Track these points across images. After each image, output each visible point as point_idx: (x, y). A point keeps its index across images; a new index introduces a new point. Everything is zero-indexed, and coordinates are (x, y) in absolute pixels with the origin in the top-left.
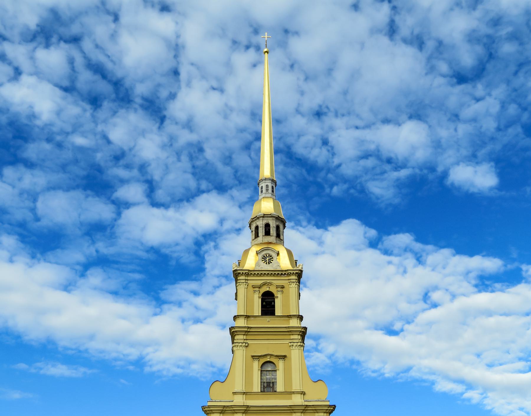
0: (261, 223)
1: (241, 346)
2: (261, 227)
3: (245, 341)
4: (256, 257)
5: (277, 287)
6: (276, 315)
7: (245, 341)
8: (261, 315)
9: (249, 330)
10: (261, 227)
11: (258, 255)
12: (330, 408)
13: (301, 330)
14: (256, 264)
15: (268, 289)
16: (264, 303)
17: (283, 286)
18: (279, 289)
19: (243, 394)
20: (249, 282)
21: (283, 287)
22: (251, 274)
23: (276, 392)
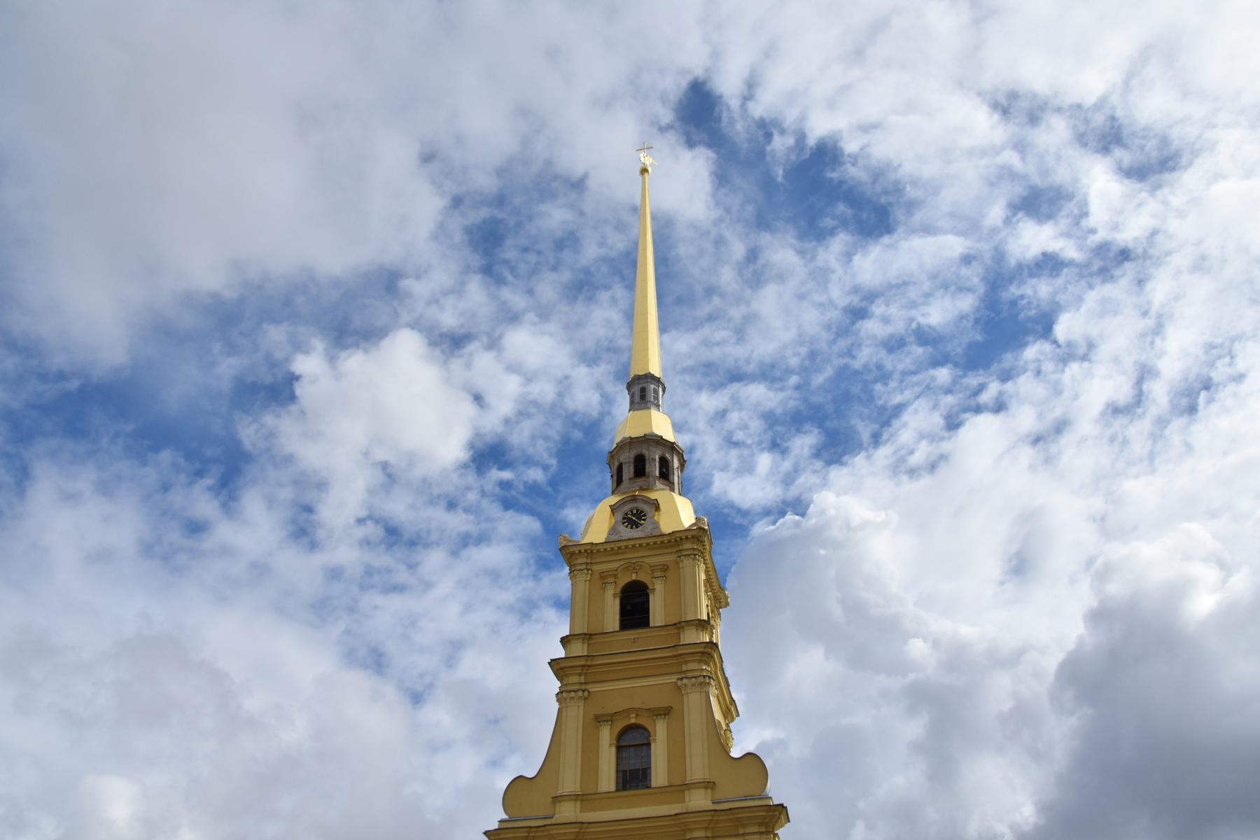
0: (627, 457)
1: (572, 698)
2: (625, 463)
3: (583, 687)
4: (611, 518)
5: (653, 568)
6: (651, 626)
7: (583, 687)
8: (617, 629)
9: (589, 663)
10: (625, 463)
11: (615, 514)
12: (771, 813)
13: (701, 650)
14: (609, 531)
15: (634, 577)
16: (629, 607)
17: (664, 565)
18: (658, 574)
19: (576, 800)
20: (595, 568)
21: (665, 568)
22: (598, 551)
23: (648, 787)
